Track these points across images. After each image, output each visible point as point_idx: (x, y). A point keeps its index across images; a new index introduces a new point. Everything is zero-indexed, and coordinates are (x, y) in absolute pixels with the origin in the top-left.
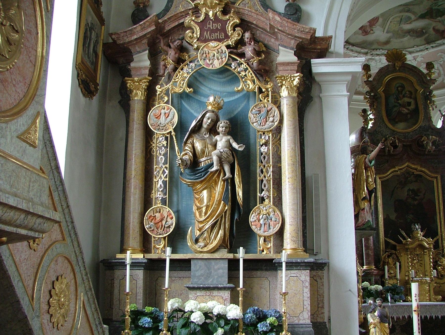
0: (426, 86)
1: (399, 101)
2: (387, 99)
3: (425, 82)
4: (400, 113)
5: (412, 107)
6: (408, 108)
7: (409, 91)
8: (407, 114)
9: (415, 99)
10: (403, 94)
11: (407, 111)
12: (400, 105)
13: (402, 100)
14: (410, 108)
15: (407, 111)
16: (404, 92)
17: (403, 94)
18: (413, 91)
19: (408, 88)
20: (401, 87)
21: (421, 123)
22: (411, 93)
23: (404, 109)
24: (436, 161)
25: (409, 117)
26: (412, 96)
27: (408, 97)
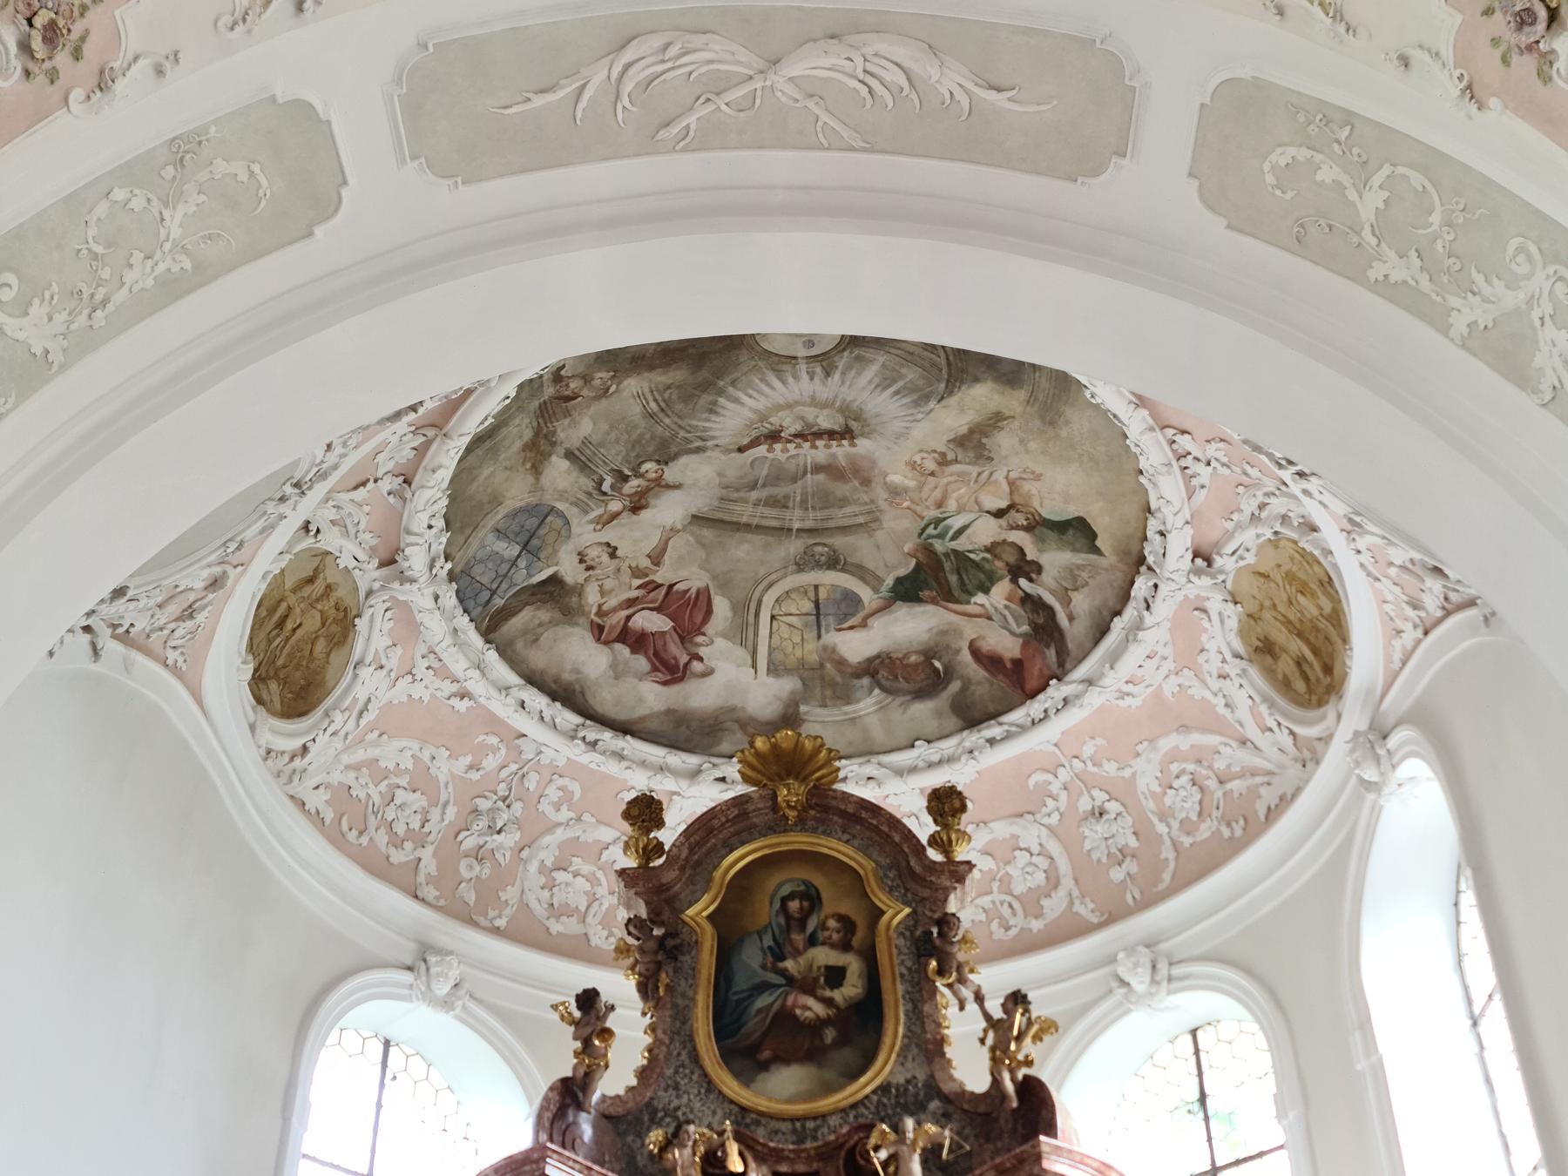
0: (926, 893)
1: (789, 964)
2: (726, 953)
3: (918, 869)
4: (785, 1018)
5: (851, 989)
6: (828, 993)
7: (842, 918)
8: (827, 1022)
9: (870, 957)
11: (819, 1009)
13: (802, 960)
14: (838, 995)
15: (819, 1009)
16: (812, 924)
19: (835, 902)
20: (802, 896)
22: (847, 924)
23: (811, 1002)
26: (856, 941)
27: (833, 946)
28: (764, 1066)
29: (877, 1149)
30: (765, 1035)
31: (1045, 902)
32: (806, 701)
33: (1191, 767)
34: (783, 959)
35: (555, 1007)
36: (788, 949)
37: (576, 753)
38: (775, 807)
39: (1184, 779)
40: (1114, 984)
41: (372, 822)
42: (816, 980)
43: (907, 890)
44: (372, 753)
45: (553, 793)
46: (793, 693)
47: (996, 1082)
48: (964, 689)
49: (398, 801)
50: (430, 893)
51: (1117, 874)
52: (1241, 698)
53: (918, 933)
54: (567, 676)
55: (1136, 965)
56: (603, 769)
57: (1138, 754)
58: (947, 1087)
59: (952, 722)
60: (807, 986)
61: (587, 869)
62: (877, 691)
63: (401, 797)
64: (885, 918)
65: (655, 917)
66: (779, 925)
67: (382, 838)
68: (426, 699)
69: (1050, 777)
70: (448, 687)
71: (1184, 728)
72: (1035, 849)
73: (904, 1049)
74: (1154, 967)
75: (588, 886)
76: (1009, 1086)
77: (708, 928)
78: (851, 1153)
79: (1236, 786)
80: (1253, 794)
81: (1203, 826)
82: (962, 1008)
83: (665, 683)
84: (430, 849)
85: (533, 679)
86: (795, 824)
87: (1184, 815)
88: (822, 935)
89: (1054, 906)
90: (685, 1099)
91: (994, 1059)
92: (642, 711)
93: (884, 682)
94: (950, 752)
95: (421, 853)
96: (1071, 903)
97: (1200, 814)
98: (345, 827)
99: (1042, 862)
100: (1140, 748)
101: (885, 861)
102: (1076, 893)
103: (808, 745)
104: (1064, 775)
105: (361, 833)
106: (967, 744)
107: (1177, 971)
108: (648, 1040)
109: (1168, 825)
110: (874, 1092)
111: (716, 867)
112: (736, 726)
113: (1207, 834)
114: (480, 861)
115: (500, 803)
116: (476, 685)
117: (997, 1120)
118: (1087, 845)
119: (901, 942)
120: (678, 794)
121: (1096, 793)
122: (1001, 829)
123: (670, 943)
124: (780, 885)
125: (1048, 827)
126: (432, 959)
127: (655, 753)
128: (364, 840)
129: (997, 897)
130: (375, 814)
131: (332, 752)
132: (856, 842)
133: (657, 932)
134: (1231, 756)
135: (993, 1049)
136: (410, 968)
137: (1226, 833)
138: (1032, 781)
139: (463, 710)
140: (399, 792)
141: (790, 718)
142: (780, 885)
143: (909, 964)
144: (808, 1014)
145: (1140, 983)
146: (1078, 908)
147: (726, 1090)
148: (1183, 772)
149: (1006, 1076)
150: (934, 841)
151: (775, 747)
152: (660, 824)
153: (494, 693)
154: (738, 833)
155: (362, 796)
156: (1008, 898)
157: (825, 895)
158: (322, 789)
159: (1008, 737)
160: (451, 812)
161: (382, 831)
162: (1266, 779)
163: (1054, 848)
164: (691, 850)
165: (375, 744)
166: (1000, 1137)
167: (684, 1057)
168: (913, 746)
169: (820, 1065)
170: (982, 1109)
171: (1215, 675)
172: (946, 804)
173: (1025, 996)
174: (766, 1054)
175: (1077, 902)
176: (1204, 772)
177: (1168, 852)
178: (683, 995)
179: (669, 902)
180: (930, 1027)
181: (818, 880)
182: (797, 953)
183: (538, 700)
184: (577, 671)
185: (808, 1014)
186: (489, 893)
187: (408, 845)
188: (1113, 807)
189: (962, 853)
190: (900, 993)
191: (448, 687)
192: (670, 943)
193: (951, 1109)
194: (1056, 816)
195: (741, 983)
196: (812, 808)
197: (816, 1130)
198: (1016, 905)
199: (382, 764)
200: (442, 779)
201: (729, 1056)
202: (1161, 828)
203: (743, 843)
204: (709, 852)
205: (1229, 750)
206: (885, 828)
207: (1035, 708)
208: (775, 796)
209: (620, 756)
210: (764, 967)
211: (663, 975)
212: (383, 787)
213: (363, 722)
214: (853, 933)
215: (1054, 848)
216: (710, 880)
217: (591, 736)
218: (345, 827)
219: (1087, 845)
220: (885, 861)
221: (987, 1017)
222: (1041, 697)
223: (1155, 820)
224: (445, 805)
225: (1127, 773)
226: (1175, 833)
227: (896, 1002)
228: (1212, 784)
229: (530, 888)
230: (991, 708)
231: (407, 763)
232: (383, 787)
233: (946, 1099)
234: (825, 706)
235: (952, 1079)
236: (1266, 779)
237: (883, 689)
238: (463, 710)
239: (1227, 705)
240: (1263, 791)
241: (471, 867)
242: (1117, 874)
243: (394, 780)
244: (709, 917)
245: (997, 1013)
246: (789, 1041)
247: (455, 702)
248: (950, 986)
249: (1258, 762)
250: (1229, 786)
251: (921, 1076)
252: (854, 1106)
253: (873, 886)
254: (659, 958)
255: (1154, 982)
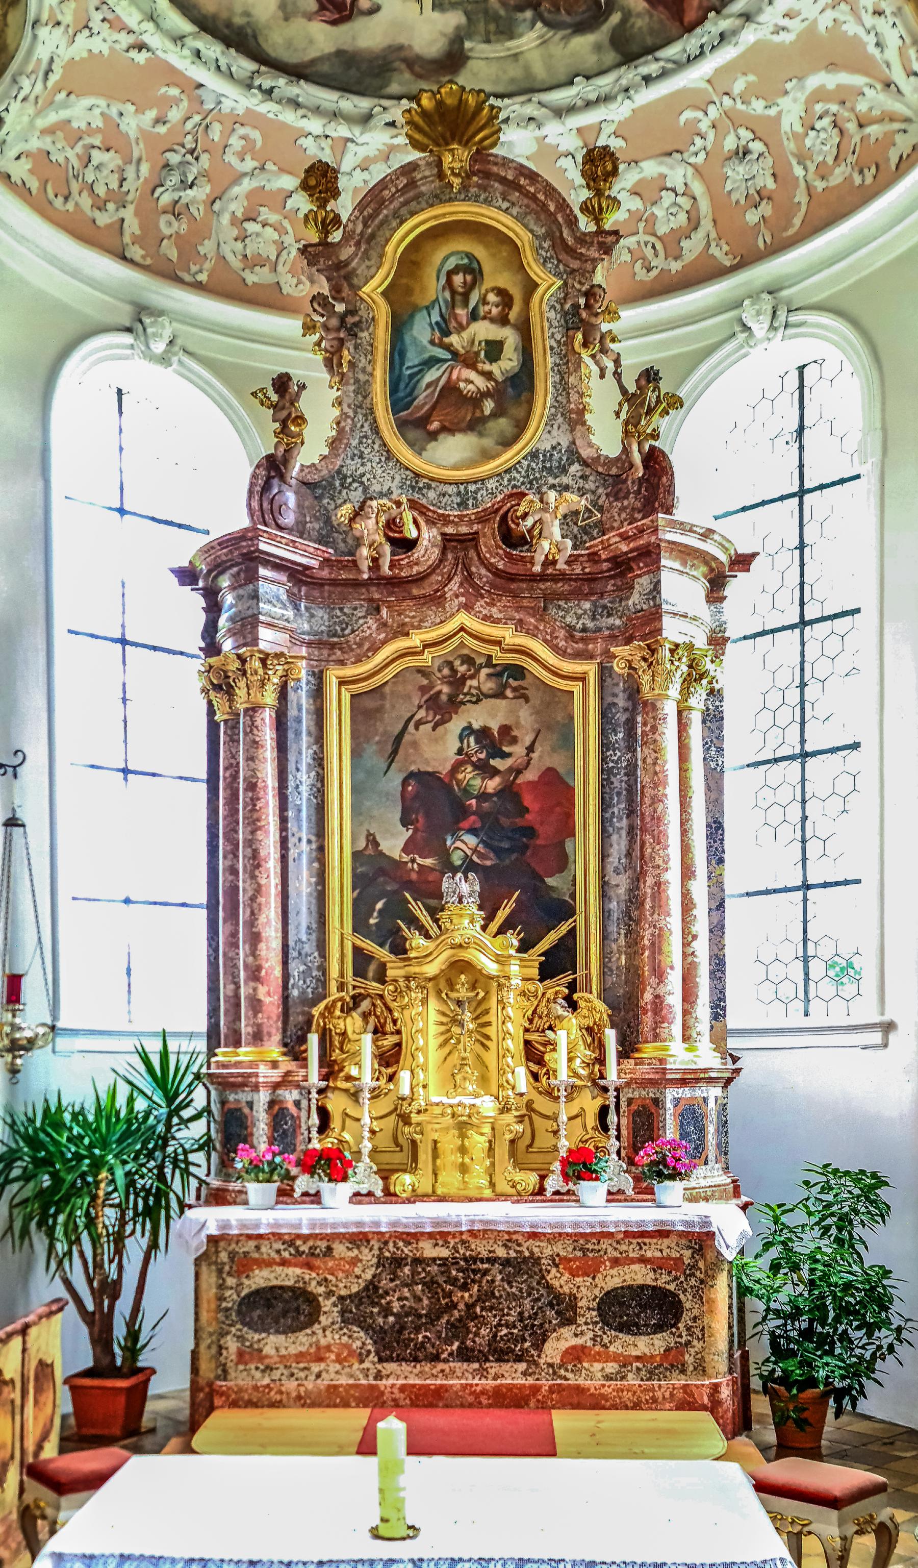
1: (454, 339)
2: (399, 326)
3: (570, 241)
4: (450, 390)
5: (509, 362)
6: (487, 367)
7: (502, 293)
8: (486, 394)
9: (524, 330)
10: (472, 304)
11: (481, 383)
12: (455, 354)
13: (465, 335)
15: (481, 383)
16: (474, 298)
17: (472, 304)
18: (516, 293)
19: (496, 276)
20: (467, 269)
21: (541, 435)
22: (506, 298)
24: (587, 605)
25: (487, 412)
26: (513, 315)
27: (493, 320)
28: (433, 436)
29: (525, 515)
30: (433, 408)
31: (685, 244)
32: (470, 36)
33: (834, 108)
34: (446, 333)
35: (254, 394)
36: (453, 324)
37: (251, 102)
38: (441, 175)
39: (826, 122)
40: (738, 329)
41: (75, 186)
42: (477, 354)
43: (559, 261)
44: (64, 114)
45: (236, 143)
46: (458, 28)
47: (626, 451)
48: (624, 21)
49: (95, 162)
50: (136, 252)
51: (752, 217)
52: (892, 39)
53: (567, 306)
54: (238, 20)
55: (758, 313)
56: (281, 117)
57: (786, 92)
58: (585, 453)
59: (611, 57)
60: (470, 361)
61: (273, 218)
62: (539, 25)
63: (98, 157)
64: (540, 290)
65: (336, 290)
66: (446, 301)
67: (86, 201)
68: (106, 52)
69: (700, 114)
70: (125, 40)
71: (832, 66)
72: (681, 189)
73: (552, 417)
74: (774, 313)
75: (276, 236)
76: (637, 458)
77: (381, 301)
78: (504, 518)
79: (873, 130)
80: (888, 141)
81: (838, 171)
82: (602, 376)
83: (334, 23)
84: (131, 208)
85: (207, 25)
86: (459, 192)
87: (821, 159)
88: (482, 310)
89: (692, 247)
90: (368, 466)
91: (626, 433)
92: (313, 53)
93: (546, 15)
94: (607, 89)
95: (123, 213)
96: (708, 245)
97: (836, 158)
98: (51, 195)
99: (684, 202)
100: (789, 86)
101: (541, 231)
102: (713, 235)
103: (471, 100)
104: (713, 111)
105: (66, 198)
106: (624, 82)
107: (794, 318)
108: (336, 412)
109: (805, 169)
110: (525, 458)
111: (387, 241)
112: (403, 66)
113: (840, 180)
114: (177, 216)
115: (189, 157)
116: (154, 39)
117: (625, 481)
118: (729, 186)
119: (552, 315)
120: (353, 141)
121: (742, 132)
122: (650, 168)
123: (350, 320)
124: (446, 258)
125: (694, 166)
126: (147, 321)
127: (327, 97)
128: (70, 206)
129: (642, 237)
130: (76, 177)
131: (26, 119)
132: (515, 211)
133: (340, 308)
134: (874, 100)
135: (626, 423)
136: (129, 330)
137: (858, 180)
138: (683, 119)
139: (142, 62)
140: (95, 154)
141: (453, 60)
142: (446, 258)
143: (558, 336)
144: (471, 387)
145: (759, 328)
146: (714, 251)
147: (402, 459)
148: (826, 113)
149: (635, 447)
150: (585, 208)
151: (440, 104)
152: (336, 194)
153: (169, 45)
154: (406, 203)
155: (61, 160)
156: (652, 239)
157: (487, 268)
158: (23, 159)
159: (664, 74)
160: (145, 169)
161: (85, 194)
162: (903, 126)
163: (698, 188)
164: (365, 225)
165: (65, 105)
166: (626, 497)
167: (366, 428)
168: (571, 83)
169: (481, 435)
170: (614, 471)
171: (871, 10)
172: (600, 165)
173: (657, 373)
174: (435, 425)
175: (713, 244)
176: (846, 114)
177: (801, 197)
178: (364, 370)
179: (348, 277)
180: (574, 397)
181: (480, 252)
182: (461, 328)
183: (213, 49)
184: (247, 14)
185: (471, 387)
186: (188, 246)
187: (111, 206)
188: (757, 147)
189: (611, 221)
190: (550, 365)
191: (125, 40)
192: (350, 320)
193: (588, 471)
194: (702, 155)
195: (413, 358)
196: (474, 174)
197: (476, 492)
198: (659, 246)
199: (75, 125)
200: (133, 134)
201: (402, 426)
202: (799, 171)
203: (413, 214)
204: (382, 224)
205: (873, 91)
206: (541, 197)
207: (691, 43)
208: (439, 164)
209: (295, 104)
210: (432, 342)
211: (346, 352)
212: (79, 149)
213: (50, 84)
214: (510, 308)
215: (698, 188)
216: (382, 255)
217: (267, 84)
218: (51, 195)
219: (729, 186)
220: (541, 231)
221: (624, 391)
222: (698, 30)
223: (794, 162)
224: (139, 161)
225: (773, 112)
226: (810, 176)
227: (546, 375)
228: (851, 127)
229: (223, 241)
230: (649, 41)
231: (98, 123)
232: (79, 149)
233: (585, 463)
234: (488, 41)
235: (590, 445)
236: (903, 126)
237: (546, 23)
238: (142, 62)
239: (878, 44)
240: (898, 138)
241: (170, 224)
242: (752, 217)
243: (88, 140)
244: (384, 294)
245: (632, 388)
246: (456, 411)
247: (133, 54)
248: (593, 356)
249: (898, 107)
250: (868, 130)
251: (565, 444)
252: (508, 471)
253: (529, 258)
254: (342, 335)
255: (772, 328)
